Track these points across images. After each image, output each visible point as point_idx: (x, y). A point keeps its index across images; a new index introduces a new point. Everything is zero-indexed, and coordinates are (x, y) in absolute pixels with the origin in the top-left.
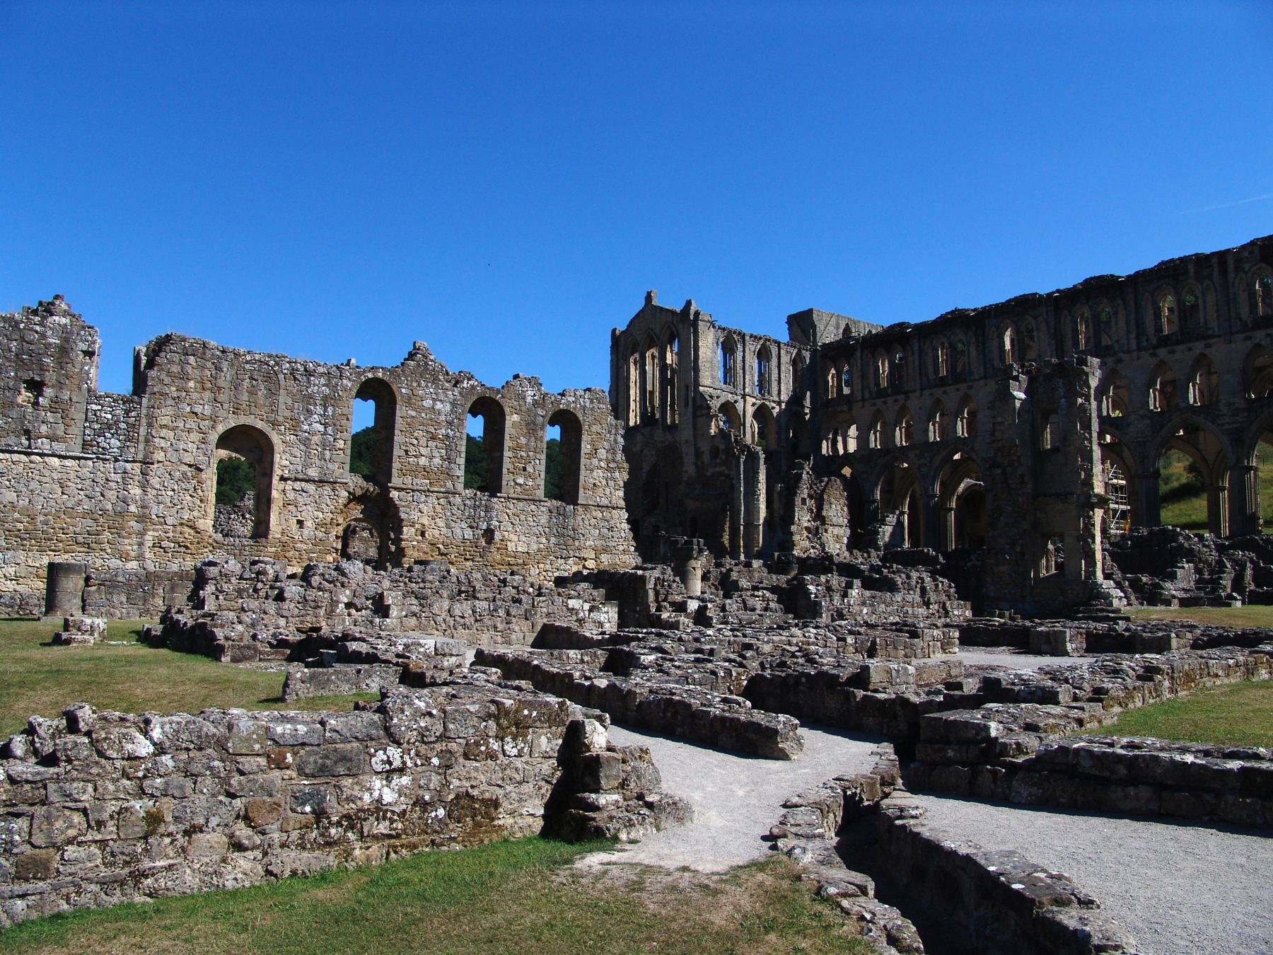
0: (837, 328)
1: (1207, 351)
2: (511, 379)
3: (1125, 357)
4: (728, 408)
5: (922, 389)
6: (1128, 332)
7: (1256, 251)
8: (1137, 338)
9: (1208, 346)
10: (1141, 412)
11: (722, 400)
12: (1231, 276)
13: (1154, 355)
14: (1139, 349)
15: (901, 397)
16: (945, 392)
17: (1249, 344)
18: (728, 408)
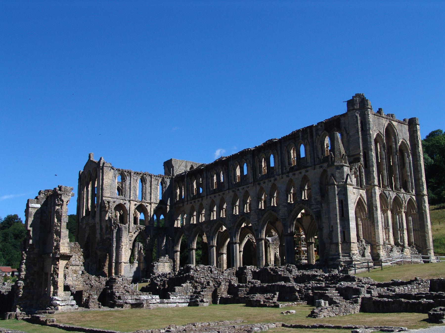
0: (186, 167)
1: (307, 174)
2: (37, 195)
3: (277, 177)
4: (120, 207)
5: (207, 195)
6: (279, 166)
7: (323, 125)
8: (282, 168)
9: (307, 171)
10: (284, 204)
11: (117, 203)
12: (315, 137)
13: (288, 176)
14: (283, 173)
15: (200, 199)
16: (215, 196)
17: (321, 170)
18: (120, 207)
